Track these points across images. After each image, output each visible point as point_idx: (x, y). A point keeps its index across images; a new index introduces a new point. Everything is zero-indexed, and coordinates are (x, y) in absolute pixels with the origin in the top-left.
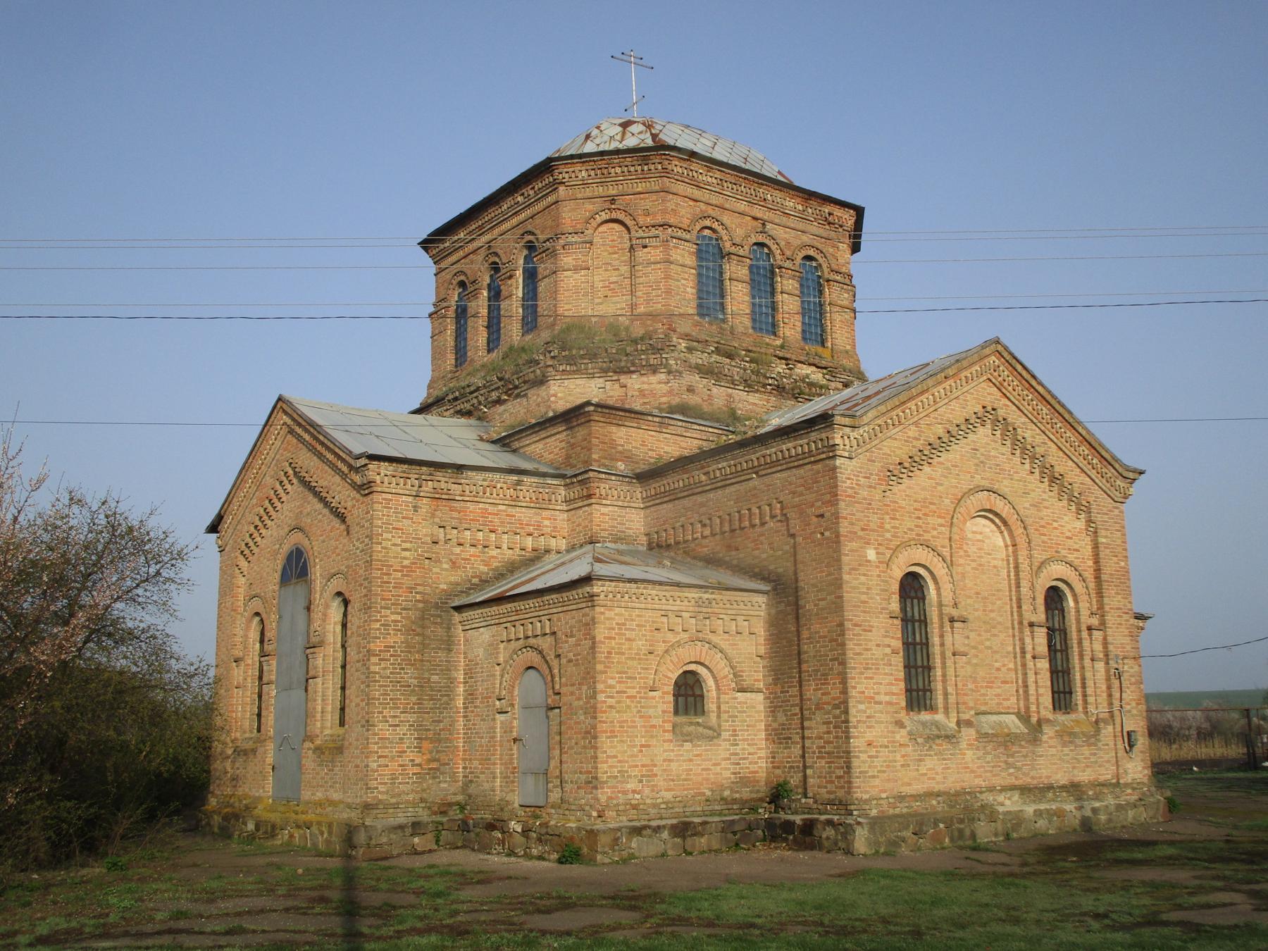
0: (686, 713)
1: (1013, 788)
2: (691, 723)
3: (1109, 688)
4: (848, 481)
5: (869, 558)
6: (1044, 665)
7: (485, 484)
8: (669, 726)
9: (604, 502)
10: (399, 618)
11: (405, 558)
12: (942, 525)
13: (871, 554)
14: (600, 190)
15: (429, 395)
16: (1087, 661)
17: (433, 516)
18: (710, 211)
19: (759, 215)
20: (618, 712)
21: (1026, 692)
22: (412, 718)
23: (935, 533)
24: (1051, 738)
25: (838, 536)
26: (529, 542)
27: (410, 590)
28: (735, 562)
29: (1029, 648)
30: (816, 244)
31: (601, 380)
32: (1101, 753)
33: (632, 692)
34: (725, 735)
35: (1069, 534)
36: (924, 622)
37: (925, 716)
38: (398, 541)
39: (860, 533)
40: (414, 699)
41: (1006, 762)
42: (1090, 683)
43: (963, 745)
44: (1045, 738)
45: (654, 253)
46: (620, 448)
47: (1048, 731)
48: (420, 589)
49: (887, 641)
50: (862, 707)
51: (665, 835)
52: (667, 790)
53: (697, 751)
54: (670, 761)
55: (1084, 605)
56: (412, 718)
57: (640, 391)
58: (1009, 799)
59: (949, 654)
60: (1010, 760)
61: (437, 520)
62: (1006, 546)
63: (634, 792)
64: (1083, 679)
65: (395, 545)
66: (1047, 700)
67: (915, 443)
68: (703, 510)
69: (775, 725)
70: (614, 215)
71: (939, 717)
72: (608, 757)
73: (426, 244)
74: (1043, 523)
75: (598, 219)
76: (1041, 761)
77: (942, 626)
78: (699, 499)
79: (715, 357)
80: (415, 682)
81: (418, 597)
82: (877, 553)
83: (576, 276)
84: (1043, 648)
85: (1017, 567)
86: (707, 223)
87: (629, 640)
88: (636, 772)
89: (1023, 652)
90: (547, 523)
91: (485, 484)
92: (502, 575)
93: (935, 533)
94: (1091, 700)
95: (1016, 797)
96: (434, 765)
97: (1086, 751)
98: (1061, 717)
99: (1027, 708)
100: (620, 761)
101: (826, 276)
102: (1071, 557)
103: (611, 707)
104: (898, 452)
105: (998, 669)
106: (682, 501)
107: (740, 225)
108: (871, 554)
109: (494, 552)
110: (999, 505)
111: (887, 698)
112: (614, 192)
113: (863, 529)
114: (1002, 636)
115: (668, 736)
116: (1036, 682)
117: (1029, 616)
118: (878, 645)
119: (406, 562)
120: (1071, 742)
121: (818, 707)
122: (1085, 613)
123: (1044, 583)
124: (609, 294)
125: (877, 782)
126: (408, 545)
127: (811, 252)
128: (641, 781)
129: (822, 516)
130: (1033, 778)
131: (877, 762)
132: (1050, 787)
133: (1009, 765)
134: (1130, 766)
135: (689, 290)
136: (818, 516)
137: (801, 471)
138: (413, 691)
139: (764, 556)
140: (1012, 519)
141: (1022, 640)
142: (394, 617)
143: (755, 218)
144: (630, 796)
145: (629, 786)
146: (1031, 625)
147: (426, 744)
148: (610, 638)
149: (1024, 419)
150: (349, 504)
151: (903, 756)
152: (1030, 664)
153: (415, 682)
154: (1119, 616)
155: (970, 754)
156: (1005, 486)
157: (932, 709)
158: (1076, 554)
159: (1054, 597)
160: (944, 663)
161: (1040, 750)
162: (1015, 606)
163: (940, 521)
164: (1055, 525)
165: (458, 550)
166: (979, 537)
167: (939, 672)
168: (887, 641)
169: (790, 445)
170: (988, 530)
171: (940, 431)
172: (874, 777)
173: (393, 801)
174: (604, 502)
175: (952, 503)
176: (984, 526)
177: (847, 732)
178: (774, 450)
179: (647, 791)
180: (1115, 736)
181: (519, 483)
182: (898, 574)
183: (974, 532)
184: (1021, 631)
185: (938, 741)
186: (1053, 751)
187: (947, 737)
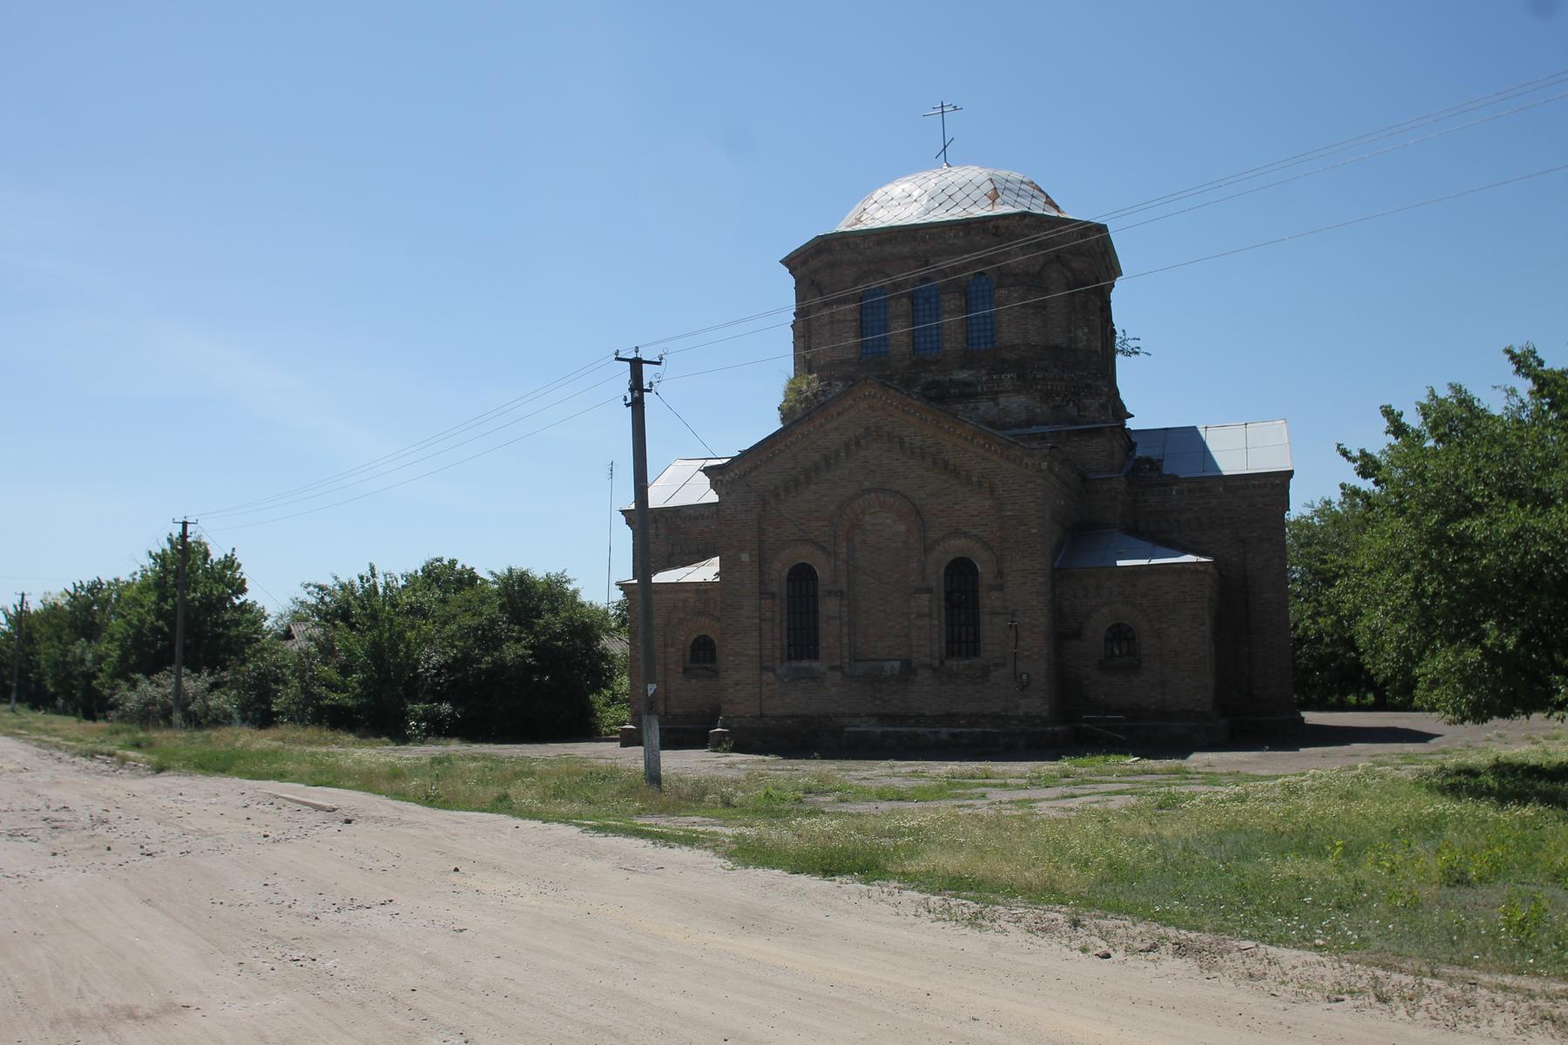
4: (728, 510)
5: (743, 560)
8: (680, 670)
13: (745, 557)
23: (817, 533)
35: (976, 513)
36: (815, 595)
50: (731, 658)
71: (815, 664)
82: (750, 556)
98: (955, 664)
102: (974, 531)
108: (745, 557)
118: (747, 618)
157: (816, 657)
163: (826, 523)
164: (957, 507)
170: (888, 521)
176: (886, 518)
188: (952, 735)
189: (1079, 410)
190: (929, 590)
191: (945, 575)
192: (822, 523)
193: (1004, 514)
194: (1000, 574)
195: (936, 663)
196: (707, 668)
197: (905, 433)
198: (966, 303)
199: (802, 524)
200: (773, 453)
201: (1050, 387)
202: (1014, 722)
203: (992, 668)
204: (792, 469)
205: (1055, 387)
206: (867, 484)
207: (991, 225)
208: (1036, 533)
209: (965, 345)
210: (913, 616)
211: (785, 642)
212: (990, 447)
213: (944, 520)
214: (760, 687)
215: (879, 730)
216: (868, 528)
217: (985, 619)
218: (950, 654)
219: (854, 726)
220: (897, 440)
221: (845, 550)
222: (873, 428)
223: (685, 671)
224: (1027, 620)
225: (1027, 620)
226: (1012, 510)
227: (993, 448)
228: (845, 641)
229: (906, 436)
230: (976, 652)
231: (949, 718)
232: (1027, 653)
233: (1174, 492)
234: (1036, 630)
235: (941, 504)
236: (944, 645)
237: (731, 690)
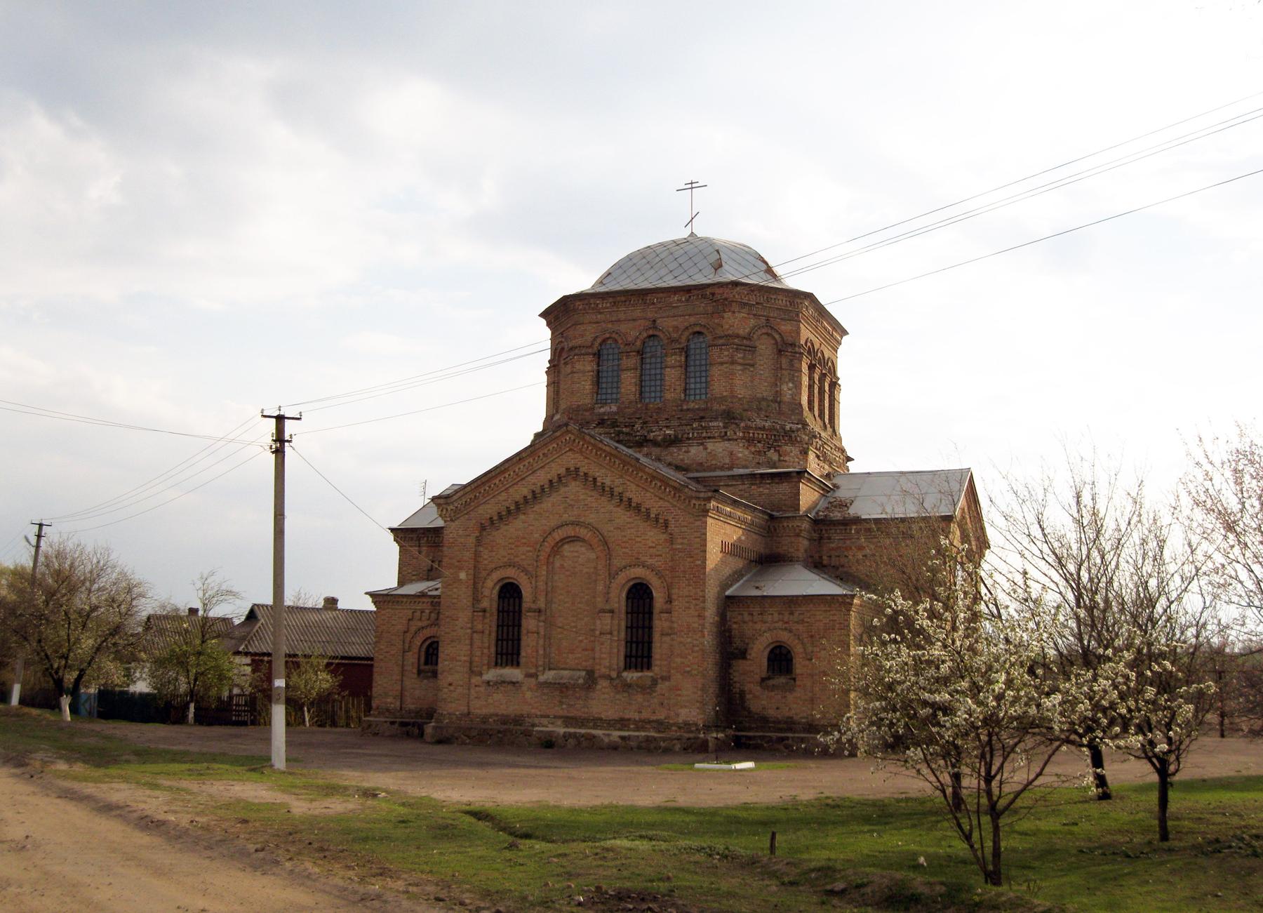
1: (560, 717)
8: (415, 671)
12: (530, 551)
13: (463, 575)
23: (524, 557)
24: (605, 688)
33: (393, 652)
38: (410, 571)
39: (457, 564)
41: (560, 702)
43: (524, 688)
44: (599, 687)
47: (602, 684)
50: (447, 663)
51: (397, 725)
52: (413, 704)
58: (552, 723)
60: (564, 700)
63: (391, 703)
67: (503, 503)
74: (625, 539)
82: (467, 575)
93: (524, 557)
95: (559, 722)
98: (632, 676)
102: (650, 561)
103: (382, 660)
104: (489, 511)
105: (581, 641)
113: (458, 561)
114: (586, 619)
115: (416, 676)
120: (623, 691)
125: (454, 705)
126: (414, 573)
127: (697, 329)
130: (584, 713)
135: (587, 387)
145: (389, 700)
151: (477, 692)
154: (687, 602)
155: (528, 695)
166: (576, 554)
172: (451, 702)
175: (541, 536)
183: (570, 551)
185: (504, 685)
186: (606, 696)
188: (623, 738)
189: (780, 456)
190: (612, 611)
191: (628, 598)
192: (528, 549)
193: (674, 546)
194: (670, 601)
195: (614, 674)
197: (598, 474)
198: (686, 357)
199: (511, 549)
200: (490, 487)
201: (751, 435)
202: (674, 728)
203: (660, 681)
204: (505, 501)
205: (756, 435)
207: (708, 292)
208: (699, 565)
209: (683, 395)
210: (598, 633)
211: (493, 650)
212: (665, 489)
213: (627, 550)
214: (469, 689)
215: (562, 730)
216: (566, 554)
217: (656, 637)
218: (628, 667)
219: (543, 726)
220: (591, 479)
221: (544, 573)
222: (572, 469)
223: (419, 672)
224: (689, 640)
225: (689, 640)
226: (682, 544)
227: (668, 490)
228: (541, 652)
229: (599, 476)
230: (649, 667)
231: (622, 723)
232: (688, 669)
233: (853, 532)
234: (696, 649)
235: (625, 536)
236: (622, 658)
237: (446, 690)
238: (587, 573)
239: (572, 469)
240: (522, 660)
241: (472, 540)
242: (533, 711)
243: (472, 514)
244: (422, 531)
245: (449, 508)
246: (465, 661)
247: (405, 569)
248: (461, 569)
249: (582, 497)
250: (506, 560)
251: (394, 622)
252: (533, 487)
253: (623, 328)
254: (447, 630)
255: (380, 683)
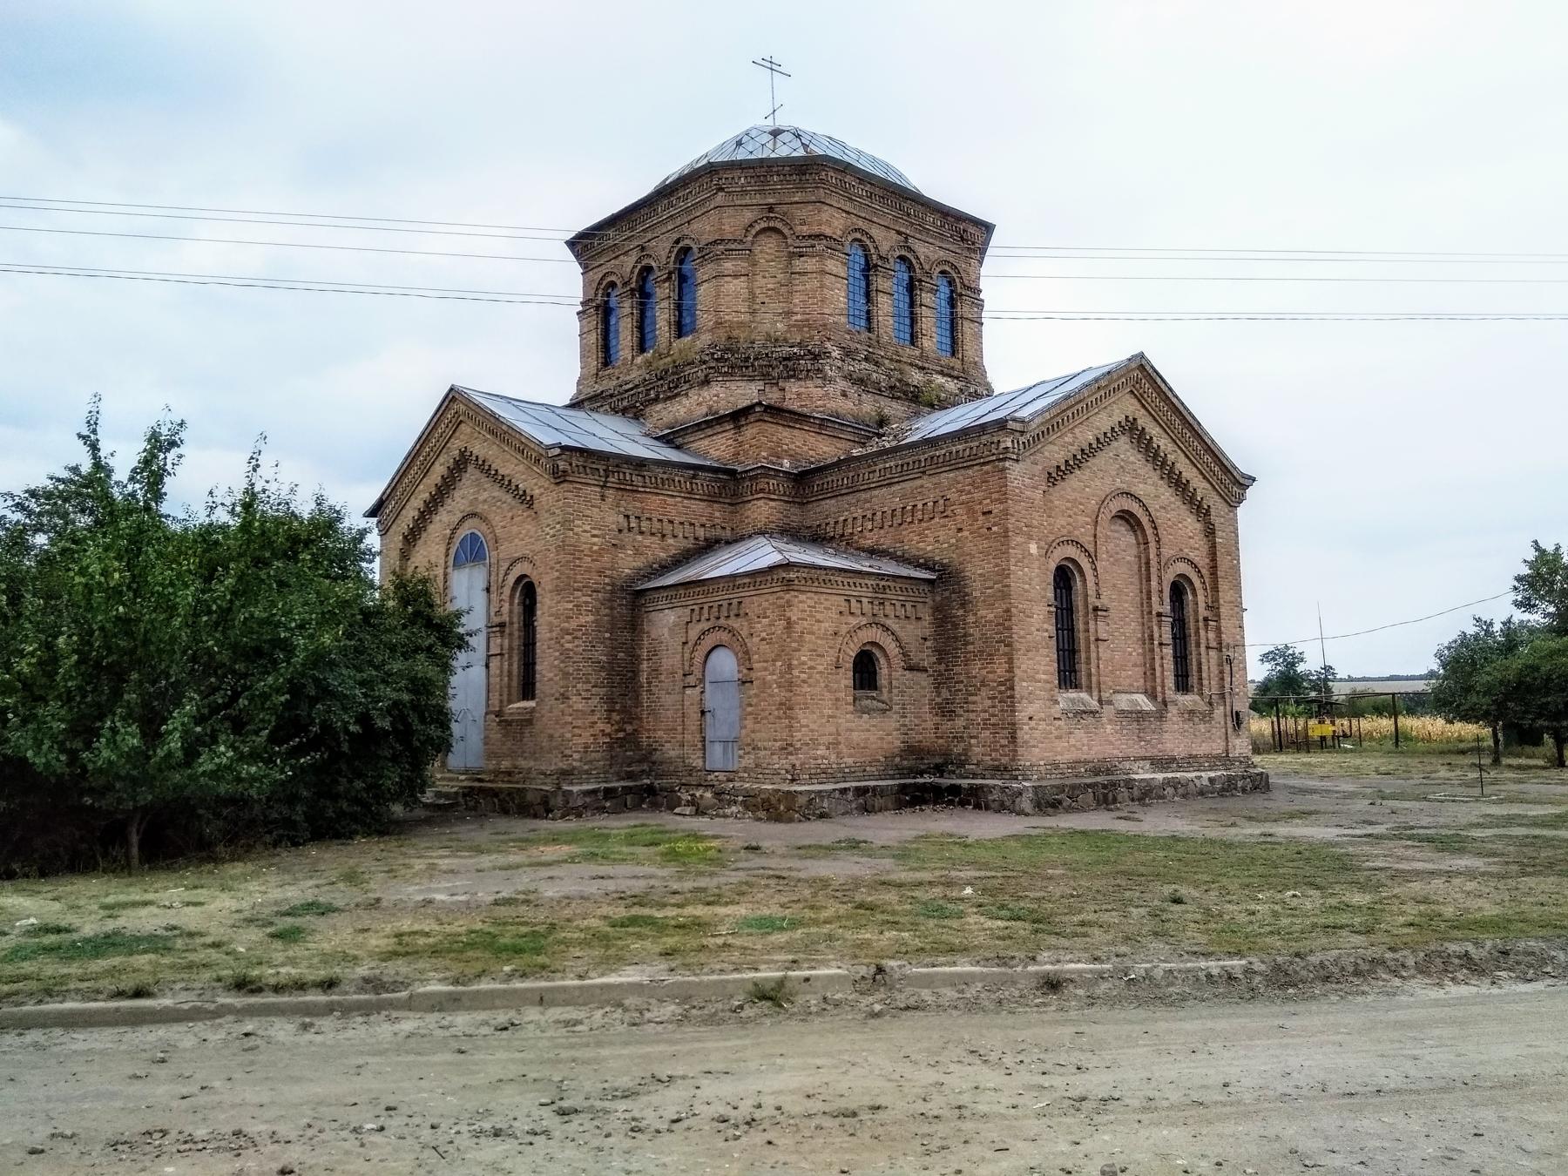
0: (862, 688)
1: (1144, 758)
2: (868, 698)
3: (1222, 672)
6: (1168, 651)
7: (665, 476)
8: (850, 699)
9: (773, 497)
10: (589, 599)
11: (594, 544)
13: (1033, 548)
14: (758, 199)
15: (579, 392)
16: (1203, 649)
17: (618, 506)
18: (861, 224)
19: (902, 229)
20: (810, 686)
21: (1153, 674)
22: (602, 691)
25: (1007, 530)
26: (701, 533)
27: (600, 573)
28: (899, 553)
29: (1156, 635)
30: (951, 260)
31: (761, 383)
32: (1214, 730)
33: (821, 668)
34: (896, 708)
37: (1072, 694)
38: (588, 528)
40: (603, 674)
42: (1205, 668)
43: (1104, 720)
45: (810, 264)
46: (785, 447)
47: (1172, 710)
48: (608, 573)
49: (1046, 626)
50: (1025, 684)
51: (850, 796)
52: (851, 756)
53: (874, 722)
54: (852, 731)
55: (1201, 598)
56: (602, 691)
57: (799, 394)
59: (1092, 638)
61: (622, 509)
62: (1139, 544)
63: (823, 757)
64: (1199, 664)
65: (585, 531)
66: (1170, 682)
68: (868, 505)
69: (939, 700)
70: (772, 224)
72: (802, 726)
73: (572, 244)
75: (758, 228)
76: (1166, 736)
77: (1087, 614)
78: (863, 495)
79: (864, 365)
80: (604, 658)
81: (607, 580)
83: (735, 281)
84: (1167, 637)
85: (1148, 563)
86: (858, 235)
87: (818, 621)
88: (824, 740)
89: (1151, 638)
90: (717, 514)
91: (665, 476)
92: (680, 561)
94: (1205, 682)
96: (621, 735)
97: (1202, 727)
99: (1154, 688)
100: (812, 731)
101: (959, 290)
103: (804, 681)
105: (1130, 654)
106: (845, 498)
107: (886, 238)
108: (1033, 548)
109: (671, 541)
110: (1135, 508)
111: (1043, 677)
112: (771, 201)
115: (851, 708)
116: (1162, 666)
117: (1156, 608)
119: (595, 548)
121: (983, 684)
122: (1202, 605)
123: (1169, 577)
124: (766, 300)
128: (828, 749)
129: (990, 512)
131: (1037, 734)
132: (1173, 759)
133: (1141, 739)
134: (1238, 742)
136: (984, 513)
137: (970, 472)
138: (603, 667)
139: (929, 548)
140: (1145, 520)
141: (1150, 628)
142: (584, 599)
143: (899, 233)
144: (820, 761)
146: (1159, 615)
147: (616, 717)
148: (802, 619)
149: (1158, 429)
150: (537, 492)
152: (1157, 650)
153: (604, 658)
156: (1139, 490)
158: (1197, 552)
159: (1178, 590)
160: (1089, 647)
161: (1166, 726)
162: (1145, 597)
165: (639, 538)
167: (1083, 655)
168: (1046, 626)
169: (960, 447)
171: (1091, 438)
173: (586, 767)
174: (773, 497)
177: (1013, 705)
178: (943, 452)
179: (833, 757)
180: (1225, 716)
181: (694, 477)
182: (1053, 566)
184: (1150, 620)
187: (1092, 712)
188: (1211, 780)
196: (873, 698)
206: (1118, 483)
215: (1160, 776)
237: (1026, 727)
238: (1128, 562)
239: (1131, 418)
240: (1084, 681)
241: (1038, 494)
242: (1116, 752)
243: (1038, 457)
244: (616, 461)
245: (1022, 439)
246: (1047, 682)
247: (577, 522)
248: (1030, 538)
249: (1132, 459)
250: (1065, 532)
251: (819, 616)
252: (1096, 432)
253: (875, 232)
254: (1022, 633)
255: (804, 722)
